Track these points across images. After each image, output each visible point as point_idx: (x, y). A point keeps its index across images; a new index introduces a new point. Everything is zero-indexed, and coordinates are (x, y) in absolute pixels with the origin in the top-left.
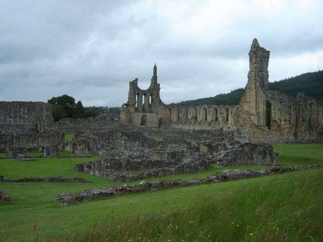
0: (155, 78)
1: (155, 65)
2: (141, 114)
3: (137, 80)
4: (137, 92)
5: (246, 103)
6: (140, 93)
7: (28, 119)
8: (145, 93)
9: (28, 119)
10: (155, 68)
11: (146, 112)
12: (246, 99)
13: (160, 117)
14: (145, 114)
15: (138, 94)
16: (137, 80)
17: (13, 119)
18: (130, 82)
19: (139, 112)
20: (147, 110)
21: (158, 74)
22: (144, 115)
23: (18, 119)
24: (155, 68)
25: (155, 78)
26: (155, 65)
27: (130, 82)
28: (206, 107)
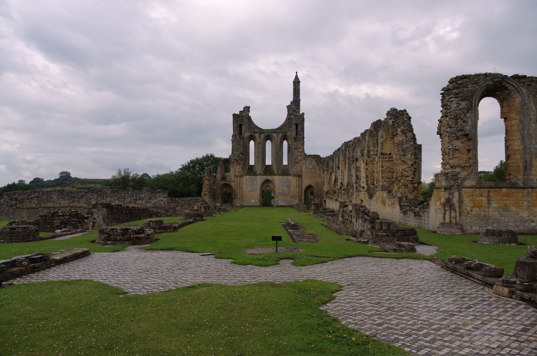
1: (297, 77)
2: (260, 179)
3: (247, 109)
4: (247, 134)
6: (257, 135)
8: (268, 135)
10: (297, 83)
11: (272, 174)
13: (306, 182)
14: (269, 178)
15: (252, 138)
16: (247, 109)
18: (234, 115)
19: (255, 174)
20: (276, 172)
22: (267, 181)
24: (297, 83)
26: (297, 76)
27: (234, 115)
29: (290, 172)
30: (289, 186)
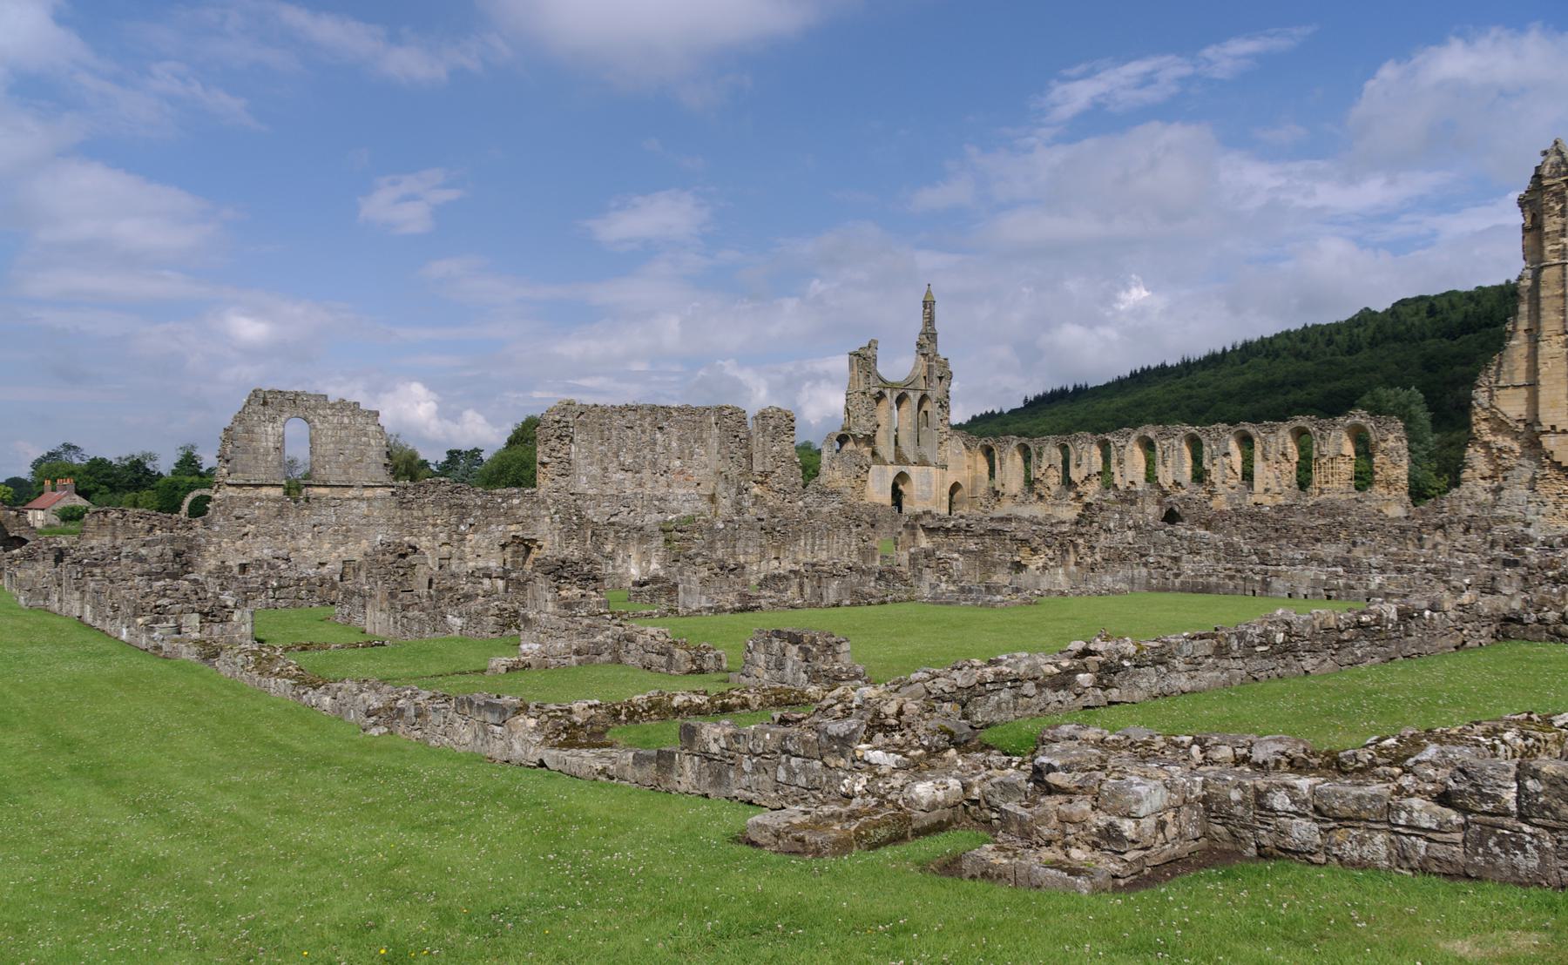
0: (928, 339)
1: (929, 293)
2: (892, 471)
3: (872, 345)
5: (1510, 391)
7: (682, 472)
9: (682, 472)
10: (928, 305)
11: (908, 464)
12: (1511, 373)
13: (951, 478)
16: (872, 345)
17: (630, 474)
19: (884, 463)
20: (912, 458)
21: (938, 326)
23: (646, 473)
24: (928, 305)
25: (928, 339)
26: (929, 293)
28: (1151, 434)
29: (930, 460)
30: (929, 484)
